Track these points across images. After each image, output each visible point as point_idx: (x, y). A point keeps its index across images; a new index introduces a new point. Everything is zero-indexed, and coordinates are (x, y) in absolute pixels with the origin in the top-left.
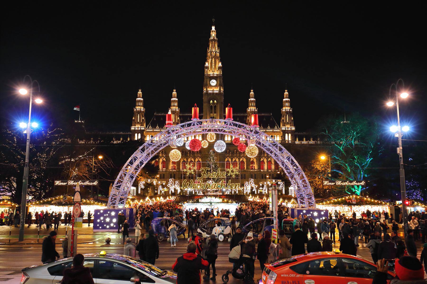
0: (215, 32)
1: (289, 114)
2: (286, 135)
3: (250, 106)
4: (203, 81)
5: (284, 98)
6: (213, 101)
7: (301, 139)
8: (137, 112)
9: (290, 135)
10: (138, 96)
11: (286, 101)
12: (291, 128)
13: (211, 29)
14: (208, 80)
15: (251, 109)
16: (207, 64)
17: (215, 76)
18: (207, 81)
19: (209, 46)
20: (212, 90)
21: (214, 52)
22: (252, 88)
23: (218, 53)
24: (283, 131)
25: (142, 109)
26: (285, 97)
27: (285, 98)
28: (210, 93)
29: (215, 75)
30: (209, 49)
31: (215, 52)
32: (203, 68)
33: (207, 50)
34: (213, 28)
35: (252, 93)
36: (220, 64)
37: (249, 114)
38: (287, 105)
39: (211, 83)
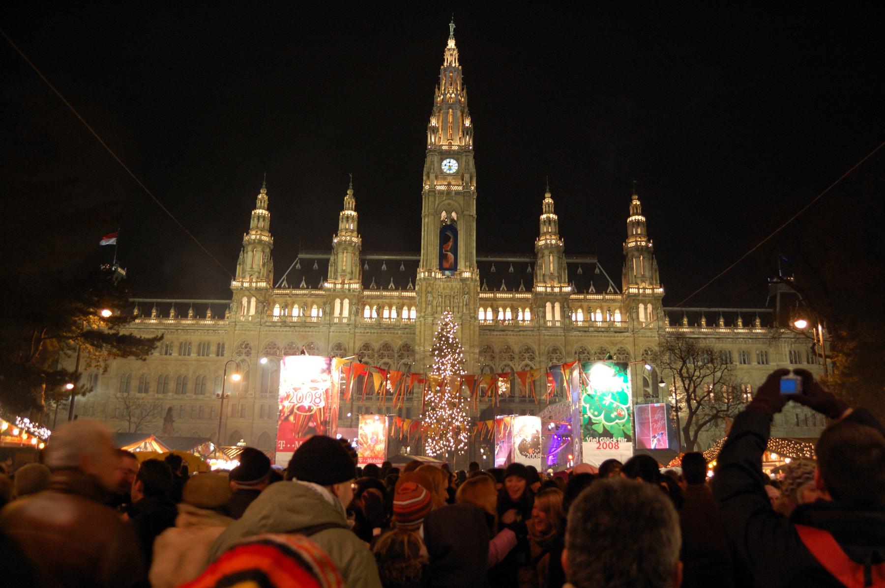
0: (456, 52)
1: (646, 255)
2: (641, 307)
3: (545, 234)
4: (423, 163)
5: (629, 216)
6: (449, 213)
7: (675, 321)
8: (250, 243)
9: (650, 306)
10: (258, 205)
11: (638, 223)
12: (653, 289)
13: (447, 45)
14: (436, 159)
15: (546, 239)
16: (434, 122)
17: (454, 151)
18: (432, 162)
19: (439, 84)
20: (446, 183)
21: (453, 95)
22: (548, 190)
23: (463, 100)
24: (629, 295)
25: (266, 238)
26: (631, 212)
27: (634, 214)
28: (441, 192)
29: (456, 148)
30: (439, 89)
31: (455, 95)
32: (423, 129)
33: (434, 93)
34: (451, 44)
35: (548, 200)
36: (467, 123)
37: (544, 254)
38: (639, 232)
39: (443, 168)
